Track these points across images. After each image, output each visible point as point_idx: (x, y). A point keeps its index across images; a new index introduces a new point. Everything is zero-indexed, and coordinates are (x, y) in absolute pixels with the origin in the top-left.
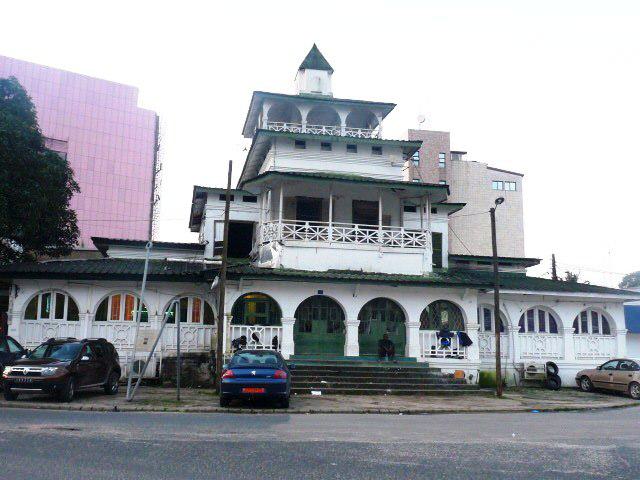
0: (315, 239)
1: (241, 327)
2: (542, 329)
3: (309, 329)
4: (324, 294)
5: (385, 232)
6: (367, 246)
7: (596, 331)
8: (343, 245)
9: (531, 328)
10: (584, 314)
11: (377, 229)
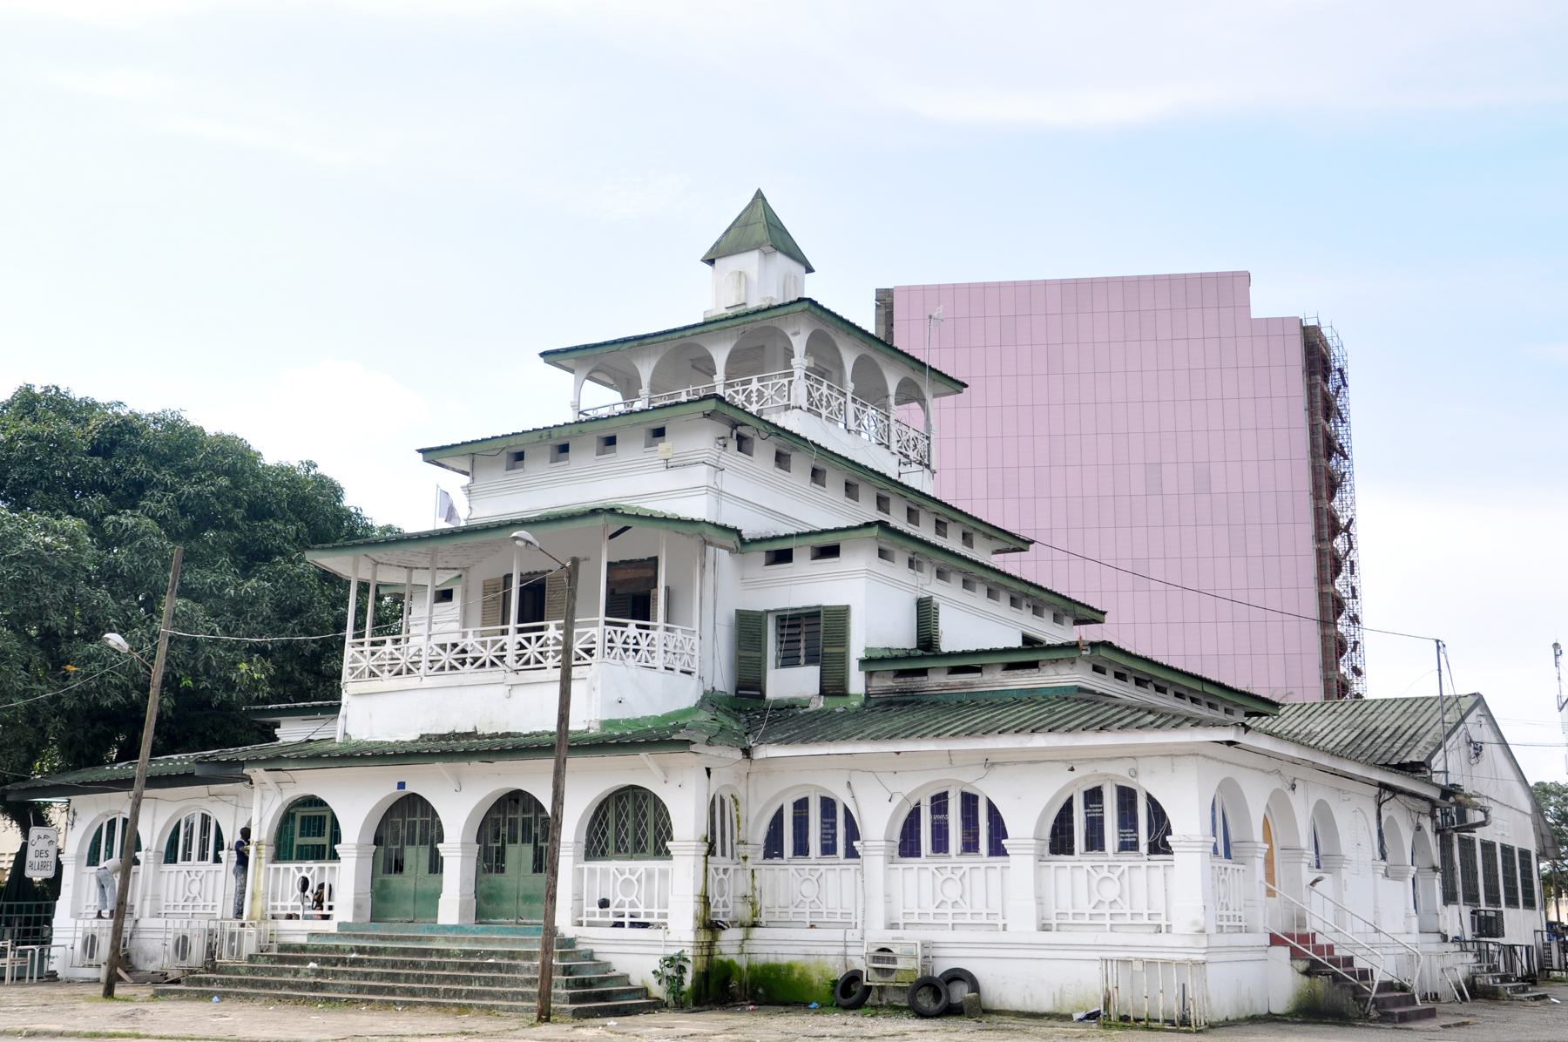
0: (399, 673)
1: (282, 866)
2: (970, 846)
3: (399, 867)
4: (409, 789)
5: (520, 637)
6: (487, 674)
7: (1128, 846)
8: (448, 678)
9: (940, 845)
10: (1093, 796)
11: (505, 632)
